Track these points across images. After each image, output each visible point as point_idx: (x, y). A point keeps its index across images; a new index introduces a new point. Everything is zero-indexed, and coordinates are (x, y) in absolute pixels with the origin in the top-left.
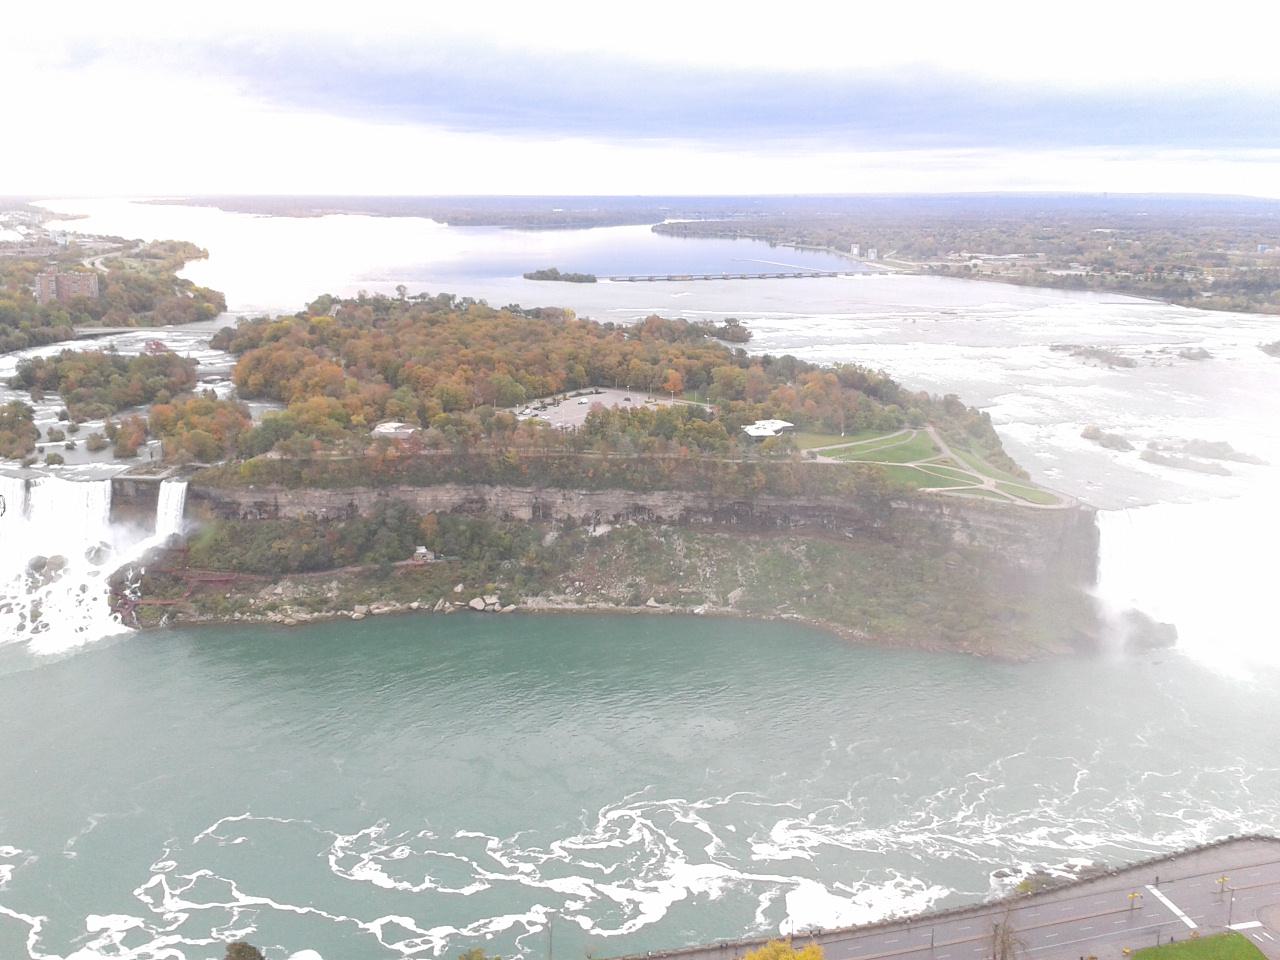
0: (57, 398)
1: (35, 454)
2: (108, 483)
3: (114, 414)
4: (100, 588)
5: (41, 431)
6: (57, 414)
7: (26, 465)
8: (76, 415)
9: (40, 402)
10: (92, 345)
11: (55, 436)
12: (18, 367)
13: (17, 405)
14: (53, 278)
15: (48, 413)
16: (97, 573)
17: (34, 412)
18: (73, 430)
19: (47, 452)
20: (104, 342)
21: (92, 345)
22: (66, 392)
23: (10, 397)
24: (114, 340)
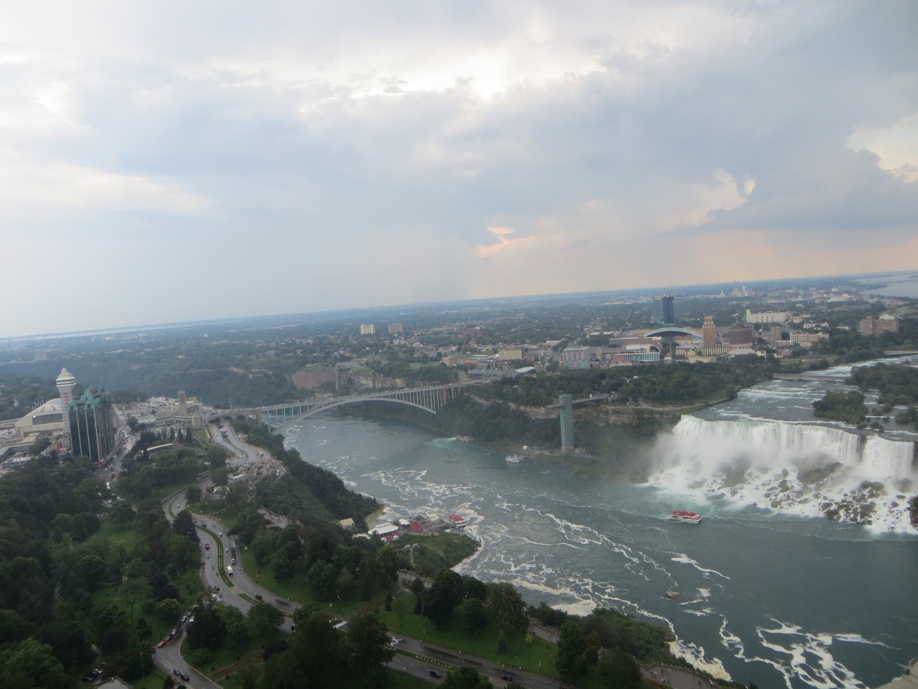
0: (876, 390)
1: (865, 422)
2: (912, 443)
3: (913, 403)
4: (904, 505)
5: (868, 409)
6: (876, 400)
7: (860, 428)
8: (887, 405)
9: (866, 392)
10: (897, 361)
11: (875, 412)
12: (852, 372)
13: (853, 393)
14: (871, 322)
15: (872, 399)
16: (902, 497)
17: (865, 397)
18: (887, 410)
19: (873, 421)
20: (904, 359)
21: (897, 361)
22: (882, 388)
23: (847, 389)
24: (909, 358)
